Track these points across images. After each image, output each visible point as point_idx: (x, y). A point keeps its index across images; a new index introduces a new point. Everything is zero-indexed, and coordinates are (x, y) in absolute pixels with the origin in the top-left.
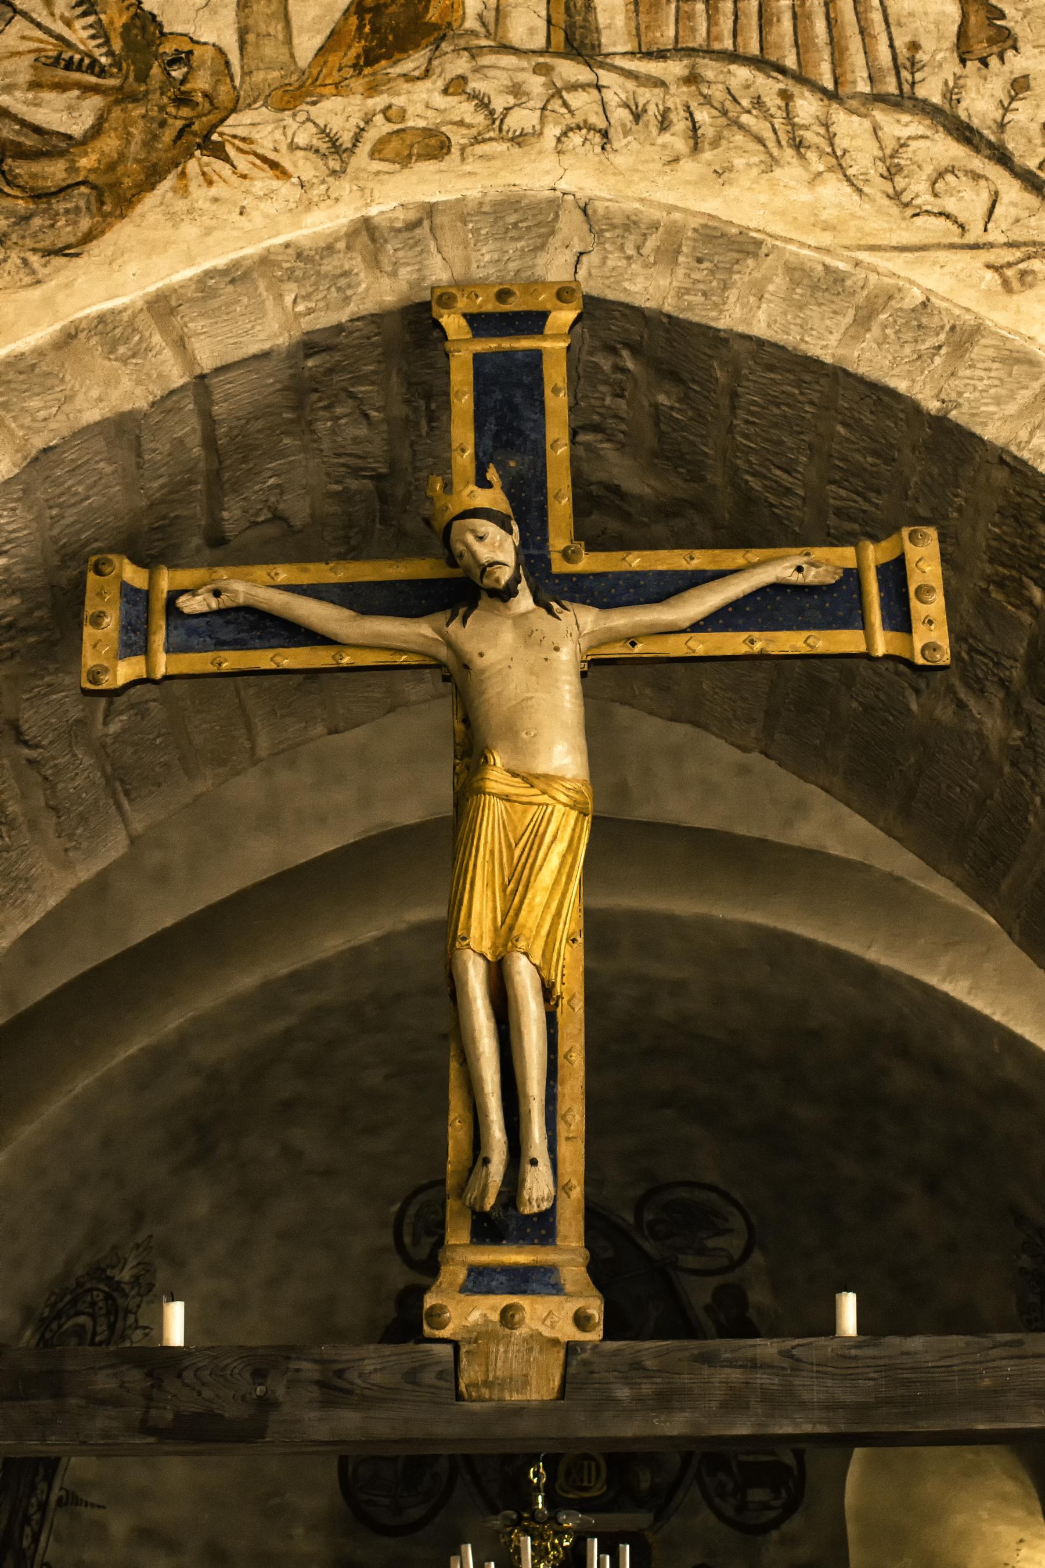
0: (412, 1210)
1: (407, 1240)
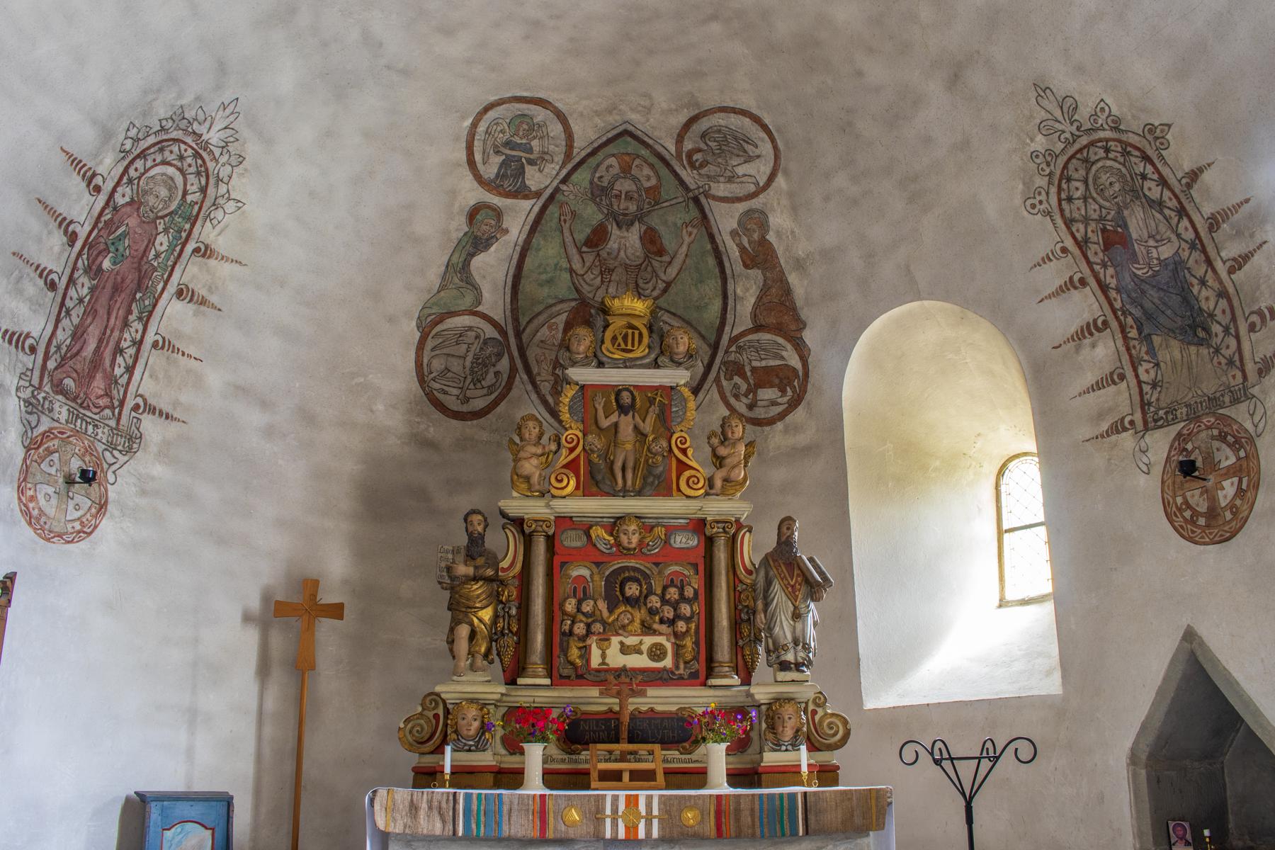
0: (482, 128)
1: (478, 157)
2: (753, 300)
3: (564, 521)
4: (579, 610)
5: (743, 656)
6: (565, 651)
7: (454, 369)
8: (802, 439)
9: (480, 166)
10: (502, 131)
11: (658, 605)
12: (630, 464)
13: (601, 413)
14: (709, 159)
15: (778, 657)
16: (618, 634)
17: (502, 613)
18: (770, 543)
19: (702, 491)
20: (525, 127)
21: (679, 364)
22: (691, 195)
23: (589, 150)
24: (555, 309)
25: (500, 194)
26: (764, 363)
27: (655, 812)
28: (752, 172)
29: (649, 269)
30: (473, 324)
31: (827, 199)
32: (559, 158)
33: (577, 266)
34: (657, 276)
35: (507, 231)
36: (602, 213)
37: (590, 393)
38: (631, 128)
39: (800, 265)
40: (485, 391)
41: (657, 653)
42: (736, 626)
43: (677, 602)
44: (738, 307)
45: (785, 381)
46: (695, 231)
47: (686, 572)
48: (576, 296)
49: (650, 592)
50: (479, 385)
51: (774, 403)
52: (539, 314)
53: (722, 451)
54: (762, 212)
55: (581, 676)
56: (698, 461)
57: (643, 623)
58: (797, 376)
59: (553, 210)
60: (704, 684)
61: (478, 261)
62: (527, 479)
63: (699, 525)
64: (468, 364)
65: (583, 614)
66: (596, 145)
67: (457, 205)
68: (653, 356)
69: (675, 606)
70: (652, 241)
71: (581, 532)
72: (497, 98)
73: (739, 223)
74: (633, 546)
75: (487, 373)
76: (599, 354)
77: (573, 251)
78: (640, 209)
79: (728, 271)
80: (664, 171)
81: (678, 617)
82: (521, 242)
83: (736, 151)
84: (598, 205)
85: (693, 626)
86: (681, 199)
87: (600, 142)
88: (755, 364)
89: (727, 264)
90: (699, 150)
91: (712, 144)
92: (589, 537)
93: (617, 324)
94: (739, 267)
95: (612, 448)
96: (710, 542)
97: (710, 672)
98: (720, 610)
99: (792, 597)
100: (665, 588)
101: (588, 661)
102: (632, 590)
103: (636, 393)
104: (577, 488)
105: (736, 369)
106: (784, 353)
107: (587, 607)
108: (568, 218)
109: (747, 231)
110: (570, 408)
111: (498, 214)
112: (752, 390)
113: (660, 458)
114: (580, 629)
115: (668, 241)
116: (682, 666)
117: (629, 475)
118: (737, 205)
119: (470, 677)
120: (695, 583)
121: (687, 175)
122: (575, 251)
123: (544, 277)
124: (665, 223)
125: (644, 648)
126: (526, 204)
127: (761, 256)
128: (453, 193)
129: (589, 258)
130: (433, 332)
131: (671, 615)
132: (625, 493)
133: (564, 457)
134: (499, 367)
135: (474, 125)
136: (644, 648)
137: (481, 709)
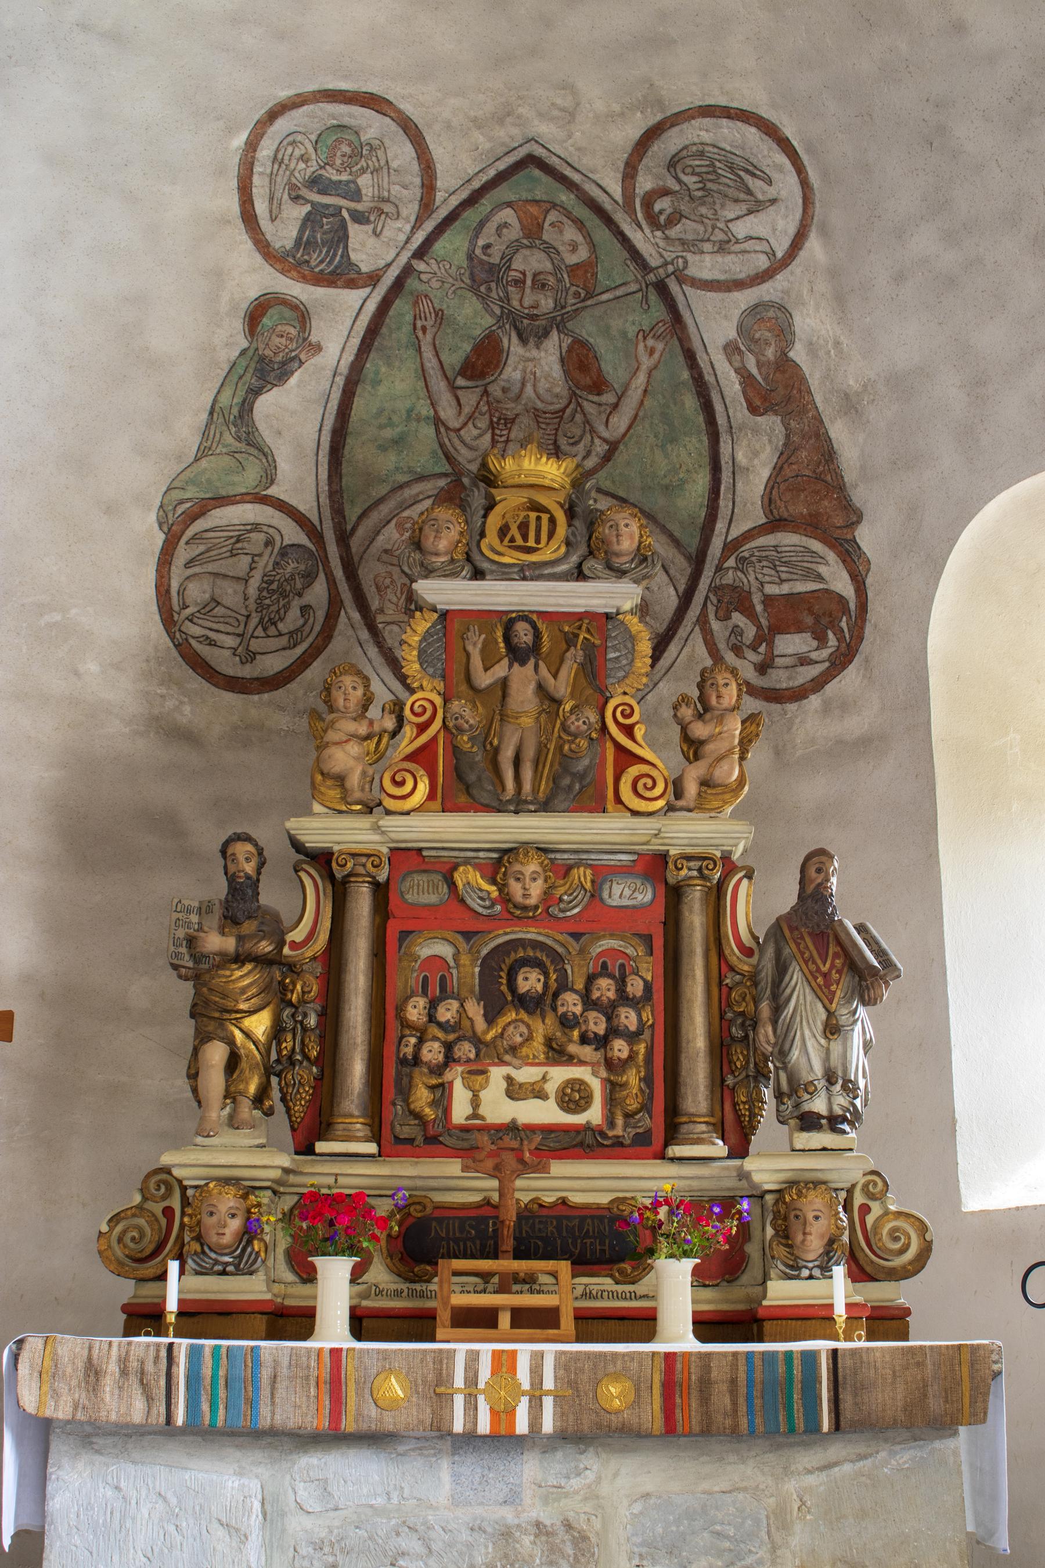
0: (265, 151)
1: (261, 207)
2: (765, 473)
3: (409, 857)
4: (432, 1018)
5: (735, 1104)
6: (405, 1092)
7: (228, 601)
8: (855, 725)
9: (265, 223)
10: (303, 158)
11: (578, 1010)
12: (529, 753)
13: (476, 662)
14: (684, 208)
15: (797, 1106)
16: (503, 1063)
17: (290, 1024)
18: (785, 897)
19: (661, 803)
20: (346, 149)
21: (621, 573)
22: (651, 277)
23: (464, 195)
24: (407, 493)
25: (304, 279)
26: (785, 589)
27: (549, 1384)
28: (762, 231)
29: (579, 417)
30: (260, 520)
31: (899, 278)
32: (410, 210)
33: (448, 412)
34: (593, 431)
35: (318, 348)
36: (492, 314)
37: (457, 625)
38: (539, 151)
39: (851, 405)
40: (284, 641)
41: (573, 1097)
42: (721, 1049)
43: (613, 1005)
44: (739, 485)
45: (825, 621)
46: (660, 346)
47: (630, 951)
48: (446, 468)
49: (564, 986)
50: (272, 631)
51: (804, 661)
52: (381, 500)
53: (700, 730)
54: (782, 308)
55: (435, 1138)
56: (658, 754)
57: (549, 1042)
58: (846, 610)
59: (401, 306)
60: (662, 1156)
61: (267, 404)
62: (340, 780)
63: (655, 865)
64: (252, 591)
65: (440, 1025)
66: (476, 184)
67: (225, 297)
68: (574, 559)
69: (609, 1011)
70: (580, 363)
71: (437, 878)
72: (291, 92)
73: (740, 329)
74: (532, 901)
75: (287, 608)
76: (476, 557)
77: (440, 386)
78: (559, 306)
79: (721, 420)
80: (602, 234)
81: (614, 1031)
82: (344, 368)
83: (731, 192)
84: (483, 299)
85: (642, 1048)
86: (634, 287)
87: (484, 178)
88: (772, 590)
89: (718, 407)
90: (665, 192)
91: (690, 180)
92: (452, 885)
93: (509, 502)
94: (740, 412)
95: (496, 725)
96: (675, 895)
97: (673, 1133)
98: (692, 1019)
99: (824, 994)
100: (590, 980)
101: (447, 1111)
102: (530, 981)
103: (542, 626)
104: (431, 796)
105: (737, 600)
106: (822, 570)
107: (447, 1012)
108: (429, 323)
109: (755, 344)
110: (422, 653)
111: (302, 315)
112: (766, 637)
113: (584, 743)
114: (432, 1052)
115: (612, 367)
116: (620, 1121)
117: (527, 774)
118: (736, 295)
119: (228, 1137)
120: (647, 970)
121: (642, 239)
122: (443, 385)
123: (388, 433)
124: (606, 332)
125: (551, 1088)
126: (353, 297)
127: (780, 390)
128: (217, 275)
129: (470, 399)
130: (190, 533)
131: (601, 1029)
132: (518, 806)
133: (408, 742)
134: (309, 598)
135: (252, 145)
136: (551, 1088)
137: (245, 1197)
